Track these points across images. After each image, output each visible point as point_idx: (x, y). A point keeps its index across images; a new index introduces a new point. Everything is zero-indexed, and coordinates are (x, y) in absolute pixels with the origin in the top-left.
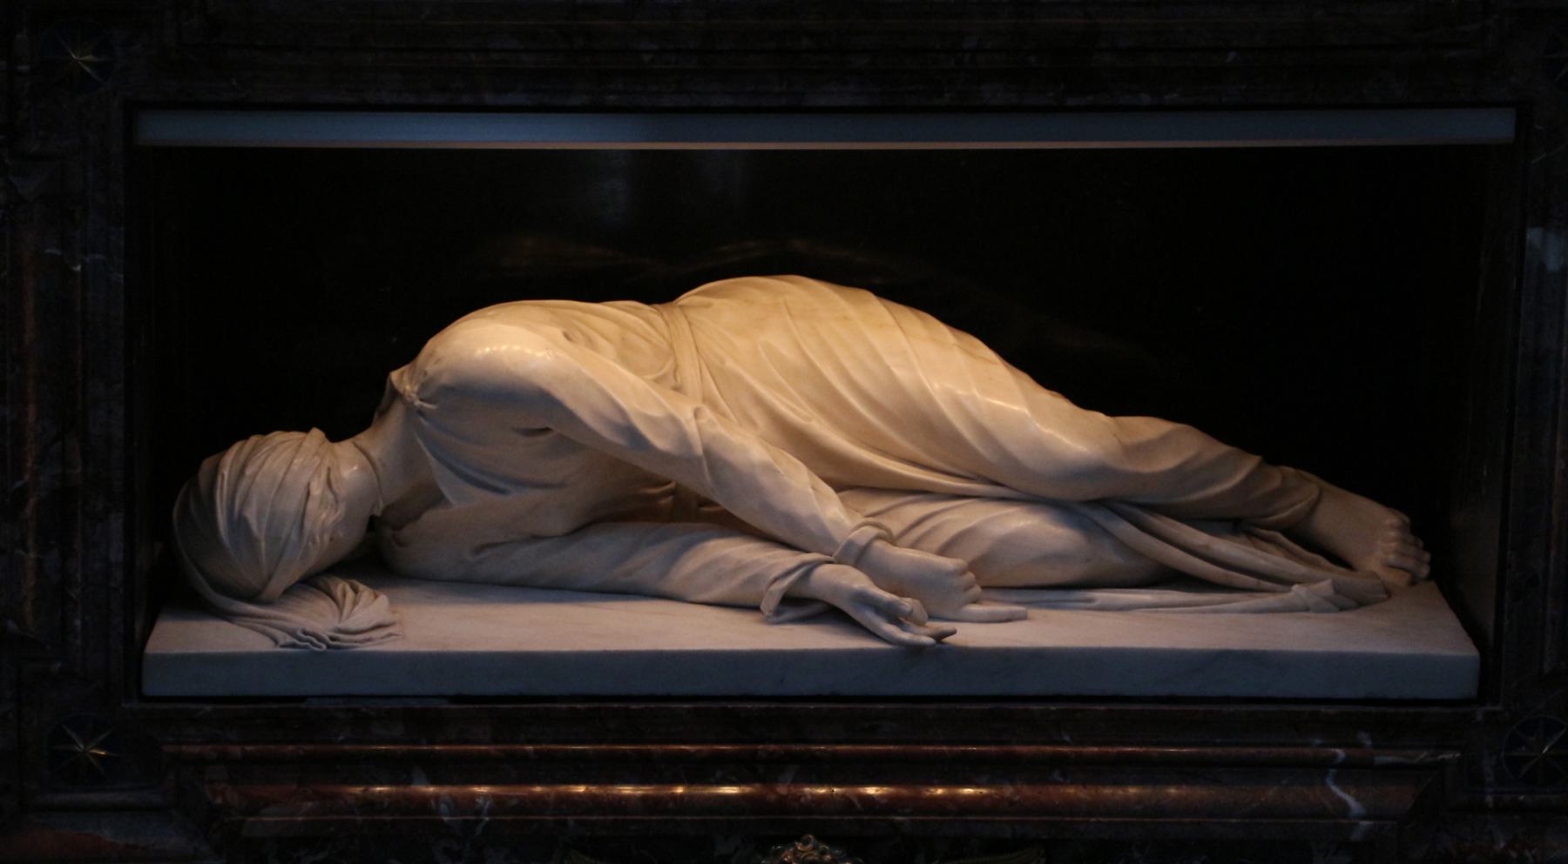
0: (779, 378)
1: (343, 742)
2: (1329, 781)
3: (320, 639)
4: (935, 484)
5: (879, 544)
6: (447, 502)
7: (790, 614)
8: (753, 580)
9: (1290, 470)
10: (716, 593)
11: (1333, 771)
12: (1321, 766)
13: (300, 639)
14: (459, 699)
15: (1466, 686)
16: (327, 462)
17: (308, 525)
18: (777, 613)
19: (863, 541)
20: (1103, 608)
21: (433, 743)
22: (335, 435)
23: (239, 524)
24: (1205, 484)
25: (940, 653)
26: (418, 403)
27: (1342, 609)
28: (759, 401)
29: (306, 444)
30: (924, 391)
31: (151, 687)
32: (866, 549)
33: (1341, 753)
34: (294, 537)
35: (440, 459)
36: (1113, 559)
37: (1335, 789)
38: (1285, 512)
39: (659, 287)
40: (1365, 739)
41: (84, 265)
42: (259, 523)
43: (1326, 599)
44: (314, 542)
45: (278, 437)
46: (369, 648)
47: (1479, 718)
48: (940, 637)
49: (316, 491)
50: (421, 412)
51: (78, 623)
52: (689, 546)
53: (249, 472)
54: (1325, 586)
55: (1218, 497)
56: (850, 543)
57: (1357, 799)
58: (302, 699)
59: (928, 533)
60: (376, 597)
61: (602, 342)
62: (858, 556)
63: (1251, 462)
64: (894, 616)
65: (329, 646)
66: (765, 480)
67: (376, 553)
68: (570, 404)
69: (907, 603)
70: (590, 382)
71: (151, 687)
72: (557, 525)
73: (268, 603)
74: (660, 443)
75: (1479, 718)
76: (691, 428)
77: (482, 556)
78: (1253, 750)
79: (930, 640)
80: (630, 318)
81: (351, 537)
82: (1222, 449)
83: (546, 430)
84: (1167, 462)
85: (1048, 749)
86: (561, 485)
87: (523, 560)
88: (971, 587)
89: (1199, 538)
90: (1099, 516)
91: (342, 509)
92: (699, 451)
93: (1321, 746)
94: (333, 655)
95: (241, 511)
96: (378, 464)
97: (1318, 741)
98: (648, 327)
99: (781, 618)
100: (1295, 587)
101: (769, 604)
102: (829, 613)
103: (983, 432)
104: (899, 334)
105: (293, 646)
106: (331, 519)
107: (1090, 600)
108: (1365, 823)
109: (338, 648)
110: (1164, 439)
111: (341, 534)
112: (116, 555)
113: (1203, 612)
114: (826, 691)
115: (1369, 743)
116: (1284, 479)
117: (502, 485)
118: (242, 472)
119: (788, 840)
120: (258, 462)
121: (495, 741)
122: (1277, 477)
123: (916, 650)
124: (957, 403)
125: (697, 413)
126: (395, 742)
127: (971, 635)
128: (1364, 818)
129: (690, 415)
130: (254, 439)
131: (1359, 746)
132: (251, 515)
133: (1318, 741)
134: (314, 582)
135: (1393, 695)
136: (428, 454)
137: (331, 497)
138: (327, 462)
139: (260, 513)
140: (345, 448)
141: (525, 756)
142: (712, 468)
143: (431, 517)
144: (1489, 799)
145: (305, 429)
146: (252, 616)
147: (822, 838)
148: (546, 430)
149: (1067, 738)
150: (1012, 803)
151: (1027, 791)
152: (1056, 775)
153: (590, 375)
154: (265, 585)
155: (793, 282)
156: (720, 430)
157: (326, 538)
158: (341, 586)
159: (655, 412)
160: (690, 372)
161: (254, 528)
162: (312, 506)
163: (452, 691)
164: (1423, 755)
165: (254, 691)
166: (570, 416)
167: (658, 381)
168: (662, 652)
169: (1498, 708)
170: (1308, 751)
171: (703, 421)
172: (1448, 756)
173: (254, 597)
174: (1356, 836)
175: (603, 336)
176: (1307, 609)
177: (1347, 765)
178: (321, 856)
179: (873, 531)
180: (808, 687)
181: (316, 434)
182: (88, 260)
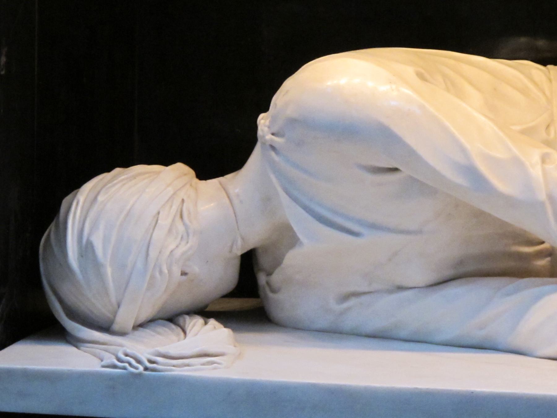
6: (301, 244)
16: (182, 194)
17: (153, 254)
26: (269, 137)
34: (140, 265)
35: (295, 200)
42: (104, 249)
44: (161, 272)
49: (165, 222)
50: (273, 148)
53: (100, 198)
60: (206, 323)
61: (469, 89)
67: (247, 297)
73: (122, 334)
77: (345, 305)
81: (219, 275)
86: (419, 232)
91: (193, 241)
95: (90, 235)
96: (236, 202)
98: (526, 81)
106: (178, 253)
111: (195, 269)
117: (356, 228)
118: (95, 198)
120: (114, 189)
130: (117, 170)
134: (172, 318)
136: (279, 189)
137: (181, 228)
138: (182, 194)
139: (106, 240)
143: (292, 259)
148: (396, 170)
154: (115, 314)
157: (177, 271)
158: (195, 324)
161: (99, 251)
162: (159, 234)
167: (528, 132)
173: (106, 327)
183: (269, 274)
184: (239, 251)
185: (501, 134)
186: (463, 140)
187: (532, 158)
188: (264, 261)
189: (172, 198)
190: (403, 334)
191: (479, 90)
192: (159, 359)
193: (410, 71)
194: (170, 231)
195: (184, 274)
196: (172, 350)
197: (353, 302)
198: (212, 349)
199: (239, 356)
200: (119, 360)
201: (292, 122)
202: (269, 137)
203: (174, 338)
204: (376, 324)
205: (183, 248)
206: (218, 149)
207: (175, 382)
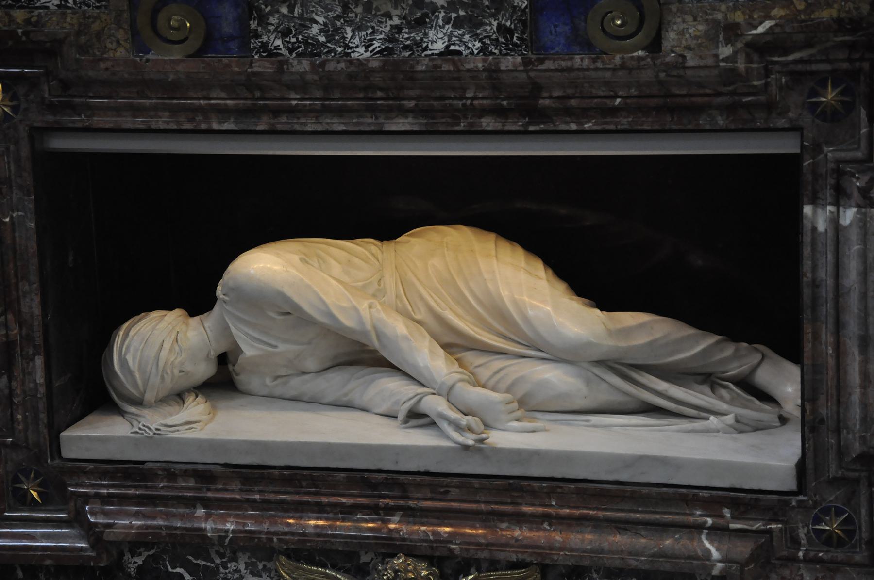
0: (437, 285)
1: (162, 488)
2: (703, 537)
3: (150, 429)
4: (508, 350)
5: (459, 384)
7: (413, 422)
8: (396, 403)
9: (745, 345)
10: (382, 409)
11: (706, 531)
12: (699, 528)
13: (140, 429)
14: (226, 465)
15: (792, 485)
16: (177, 329)
17: (161, 364)
18: (405, 422)
19: (450, 383)
20: (595, 426)
21: (209, 490)
22: (193, 313)
23: (124, 363)
24: (673, 353)
25: (478, 450)
26: (222, 296)
27: (741, 432)
28: (422, 298)
29: (166, 318)
30: (500, 295)
31: (67, 453)
32: (452, 387)
33: (710, 521)
34: (154, 370)
36: (604, 396)
37: (708, 545)
38: (735, 370)
39: (387, 229)
40: (727, 513)
41: (12, 218)
43: (731, 426)
45: (156, 314)
46: (176, 435)
47: (794, 503)
48: (482, 441)
49: (167, 346)
50: (225, 302)
51: (19, 416)
52: (373, 380)
53: (131, 333)
54: (730, 419)
55: (682, 361)
56: (443, 383)
57: (718, 549)
58: (143, 463)
59: (502, 378)
62: (448, 393)
63: (711, 339)
64: (458, 428)
65: (155, 434)
66: (404, 345)
67: (223, 380)
68: (296, 299)
69: (464, 420)
70: (308, 286)
71: (67, 453)
72: (311, 364)
73: (150, 406)
74: (348, 322)
75: (794, 503)
76: (365, 314)
77: (275, 383)
78: (658, 516)
79: (470, 442)
80: (374, 249)
82: (691, 331)
83: (289, 313)
84: (641, 340)
85: (540, 510)
87: (296, 385)
88: (514, 411)
89: (662, 385)
90: (597, 371)
92: (369, 327)
93: (701, 515)
94: (156, 439)
97: (698, 513)
99: (410, 424)
100: (712, 418)
101: (401, 416)
102: (433, 424)
103: (527, 320)
104: (495, 261)
105: (137, 432)
106: (177, 362)
107: (588, 421)
108: (719, 564)
109: (159, 434)
110: (641, 326)
112: (40, 378)
113: (654, 431)
114: (422, 470)
115: (729, 515)
116: (737, 350)
119: (394, 556)
121: (241, 490)
122: (729, 350)
123: (466, 447)
124: (515, 302)
125: (370, 307)
126: (189, 489)
127: (499, 439)
128: (720, 561)
129: (365, 304)
131: (723, 517)
132: (129, 358)
133: (698, 513)
134: (179, 397)
135: (747, 487)
137: (177, 348)
139: (134, 358)
140: (197, 318)
141: (255, 501)
142: (378, 336)
144: (801, 554)
145: (171, 309)
146: (132, 414)
147: (407, 555)
149: (554, 503)
150: (517, 540)
151: (528, 534)
152: (546, 525)
153: (309, 282)
155: (454, 229)
156: (383, 316)
157: (176, 371)
159: (345, 304)
160: (390, 282)
162: (164, 354)
163: (222, 462)
164: (758, 525)
165: (118, 457)
166: (297, 308)
168: (291, 443)
169: (805, 498)
170: (691, 519)
171: (373, 310)
172: (773, 526)
173: (139, 403)
174: (715, 572)
175: (336, 260)
176: (718, 431)
177: (713, 529)
178: (151, 553)
179: (458, 376)
180: (412, 467)
181: (178, 313)
182: (14, 215)
183: (234, 365)
184: (213, 354)
185: (346, 292)
186: (324, 298)
187: (363, 306)
188: (231, 357)
189: (171, 331)
190: (306, 399)
191: (339, 263)
192: (161, 428)
193: (296, 258)
194: (171, 350)
195: (181, 371)
196: (170, 421)
197: (279, 381)
198: (193, 419)
199: (211, 420)
200: (140, 429)
201: (233, 289)
202: (222, 296)
203: (177, 408)
204: (292, 393)
205: (179, 359)
206: (198, 300)
207: (173, 439)
